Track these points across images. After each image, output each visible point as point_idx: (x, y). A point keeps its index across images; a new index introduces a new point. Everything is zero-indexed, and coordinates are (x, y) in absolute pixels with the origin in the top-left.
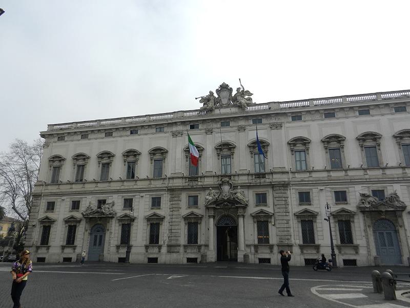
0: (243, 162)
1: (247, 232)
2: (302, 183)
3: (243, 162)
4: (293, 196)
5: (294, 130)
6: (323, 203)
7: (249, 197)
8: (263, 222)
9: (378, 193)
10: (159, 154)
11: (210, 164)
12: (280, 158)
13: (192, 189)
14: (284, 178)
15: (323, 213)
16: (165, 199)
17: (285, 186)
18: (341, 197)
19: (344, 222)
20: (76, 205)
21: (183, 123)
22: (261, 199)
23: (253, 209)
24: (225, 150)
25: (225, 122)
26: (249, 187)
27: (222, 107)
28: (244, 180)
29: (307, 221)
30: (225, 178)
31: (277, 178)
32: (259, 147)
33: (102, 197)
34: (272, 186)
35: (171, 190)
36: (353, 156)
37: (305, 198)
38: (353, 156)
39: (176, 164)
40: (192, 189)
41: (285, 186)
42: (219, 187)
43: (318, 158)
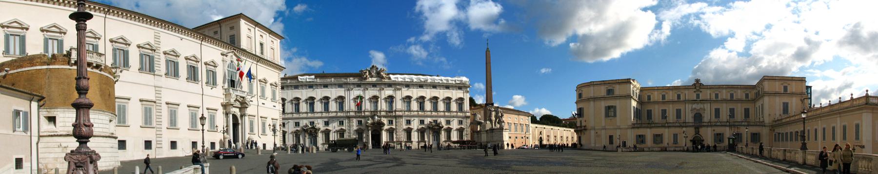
0: (383, 106)
1: (385, 137)
2: (407, 116)
3: (383, 106)
4: (403, 121)
5: (406, 92)
6: (415, 125)
7: (385, 121)
8: (391, 132)
9: (435, 121)
10: (341, 100)
11: (367, 106)
12: (399, 105)
13: (359, 117)
14: (401, 114)
15: (415, 128)
16: (346, 122)
17: (401, 117)
18: (422, 122)
19: (422, 132)
20: (297, 124)
21: (353, 84)
22: (391, 122)
23: (386, 127)
24: (375, 99)
25: (374, 85)
26: (384, 117)
27: (372, 77)
28: (383, 113)
29: (409, 131)
30: (374, 113)
31: (397, 113)
32: (390, 99)
33: (311, 120)
34: (396, 117)
35: (349, 118)
36: (428, 106)
37: (409, 122)
38: (428, 106)
39: (350, 105)
40: (359, 117)
41: (401, 117)
42: (373, 117)
43: (415, 106)
